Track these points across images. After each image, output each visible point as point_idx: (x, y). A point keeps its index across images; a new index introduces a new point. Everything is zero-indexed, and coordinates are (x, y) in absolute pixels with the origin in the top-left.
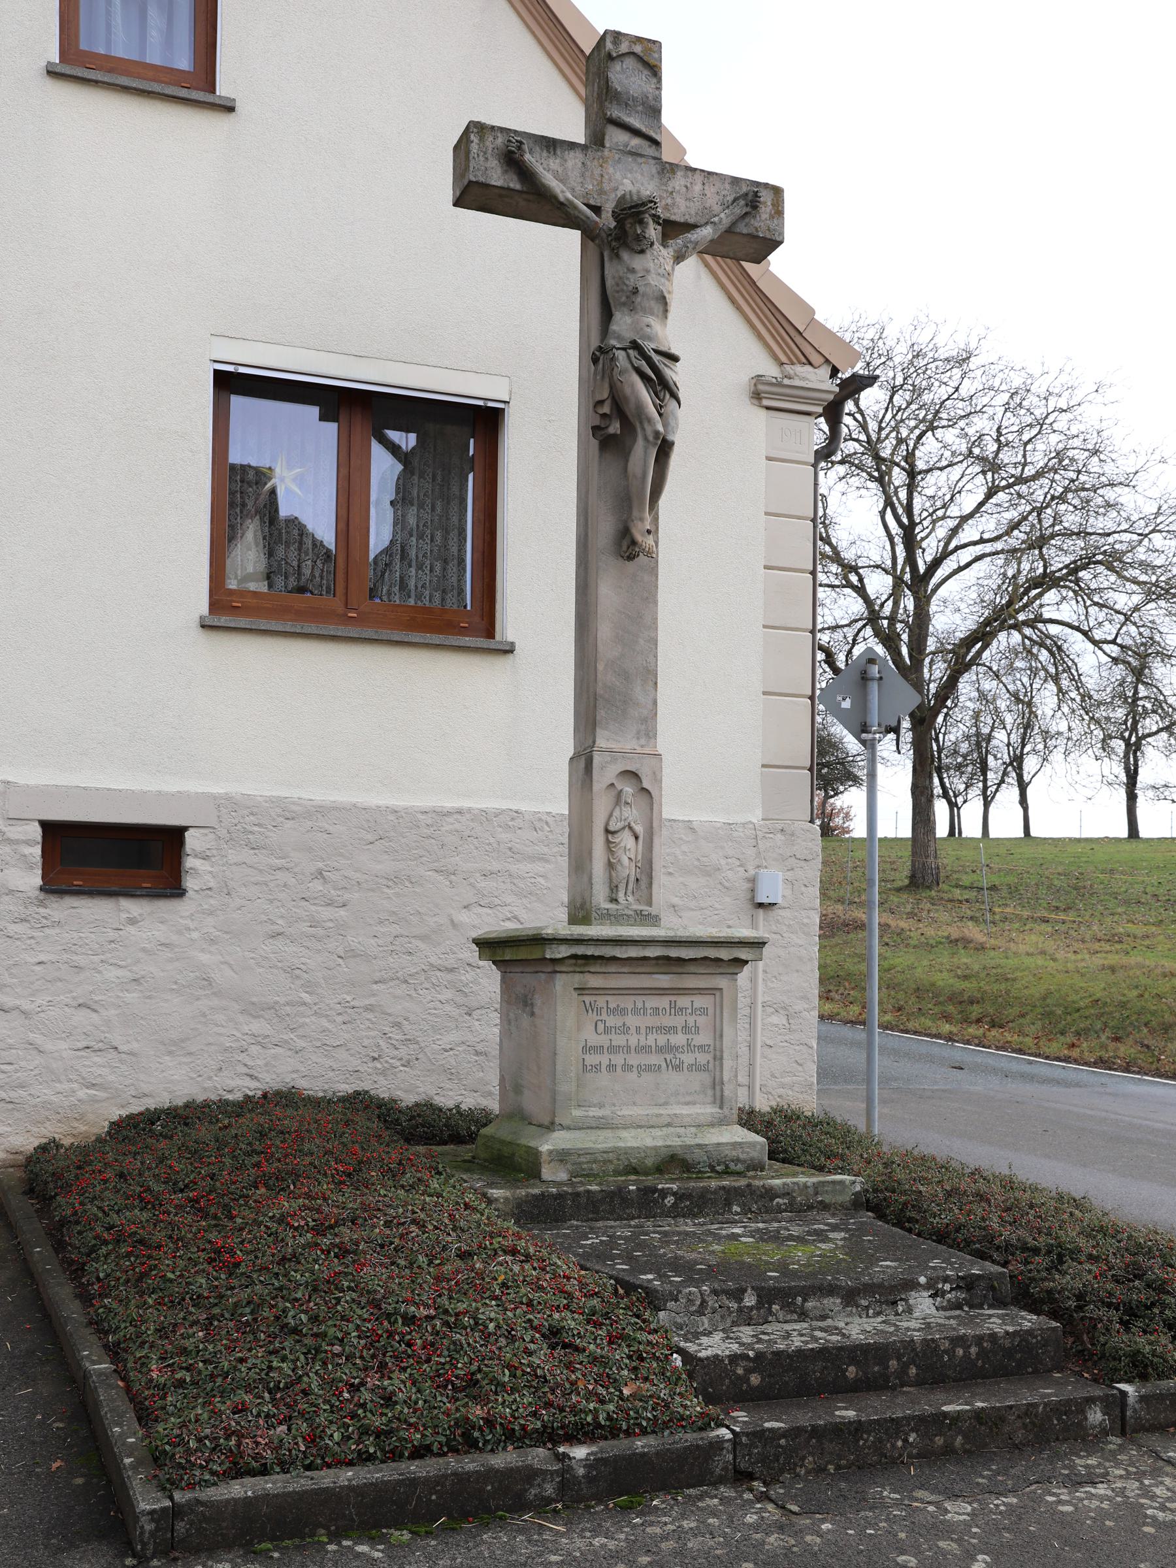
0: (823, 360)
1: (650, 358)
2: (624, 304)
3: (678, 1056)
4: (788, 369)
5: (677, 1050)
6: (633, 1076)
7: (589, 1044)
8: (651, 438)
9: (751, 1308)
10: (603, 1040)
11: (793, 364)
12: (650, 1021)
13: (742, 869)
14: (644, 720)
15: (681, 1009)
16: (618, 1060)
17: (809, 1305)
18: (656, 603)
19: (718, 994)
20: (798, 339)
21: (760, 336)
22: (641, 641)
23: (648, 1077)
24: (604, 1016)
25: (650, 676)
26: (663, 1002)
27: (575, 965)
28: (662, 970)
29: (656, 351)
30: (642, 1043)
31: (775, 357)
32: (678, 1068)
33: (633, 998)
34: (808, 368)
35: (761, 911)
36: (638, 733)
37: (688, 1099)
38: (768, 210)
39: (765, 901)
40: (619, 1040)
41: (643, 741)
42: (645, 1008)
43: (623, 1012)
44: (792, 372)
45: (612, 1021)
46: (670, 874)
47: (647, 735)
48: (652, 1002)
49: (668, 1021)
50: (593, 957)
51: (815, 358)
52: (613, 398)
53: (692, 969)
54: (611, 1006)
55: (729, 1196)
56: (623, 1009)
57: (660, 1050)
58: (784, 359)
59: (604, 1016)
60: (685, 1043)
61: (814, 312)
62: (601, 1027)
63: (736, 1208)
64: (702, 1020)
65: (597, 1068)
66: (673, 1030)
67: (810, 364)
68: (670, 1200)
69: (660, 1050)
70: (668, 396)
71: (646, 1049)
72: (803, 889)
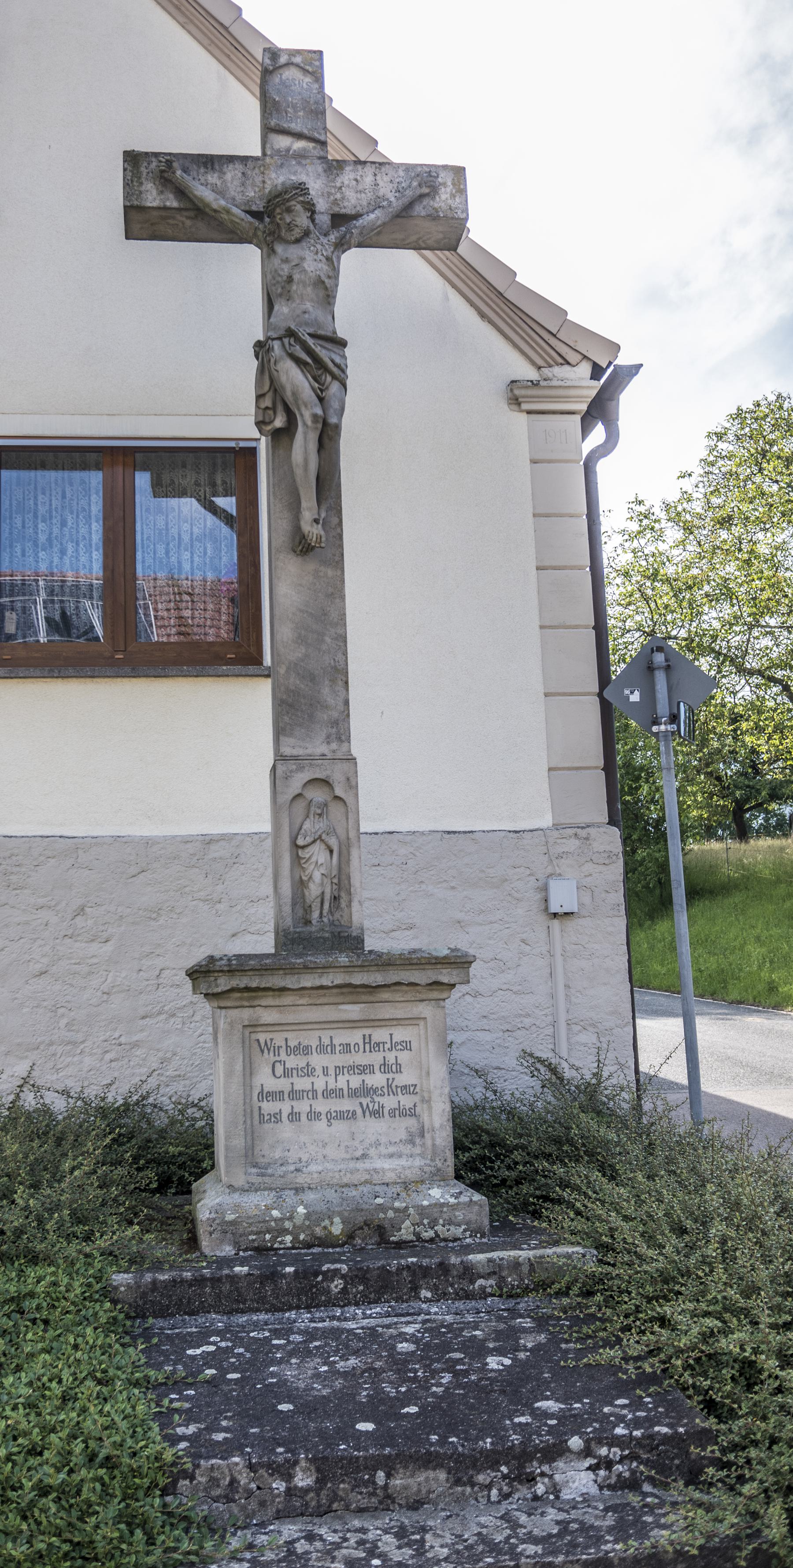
0: (580, 357)
1: (305, 341)
2: (281, 295)
3: (377, 1099)
4: (546, 372)
5: (375, 1092)
6: (321, 1125)
7: (295, 1088)
8: (309, 423)
9: (306, 1490)
10: (283, 1084)
11: (550, 366)
12: (340, 1059)
13: (533, 878)
14: (335, 723)
15: (378, 1044)
16: (303, 1107)
17: (397, 1482)
18: (343, 598)
19: (422, 1023)
20: (553, 341)
21: (515, 346)
22: (328, 639)
23: (340, 1128)
24: (283, 1056)
25: (340, 675)
26: (355, 1037)
27: (241, 999)
28: (347, 999)
29: (312, 335)
30: (332, 1086)
31: (533, 363)
32: (377, 1113)
33: (318, 1033)
34: (567, 368)
35: (556, 923)
36: (328, 737)
37: (392, 1149)
38: (448, 190)
39: (560, 911)
40: (302, 1084)
41: (334, 746)
42: (333, 1046)
43: (306, 1050)
44: (550, 375)
45: (292, 1062)
46: (453, 888)
47: (339, 739)
48: (342, 1037)
49: (361, 1059)
50: (257, 989)
51: (572, 357)
52: (275, 390)
53: (385, 995)
54: (292, 1043)
55: (420, 1274)
56: (307, 1047)
57: (354, 1093)
58: (540, 362)
59: (283, 1056)
60: (385, 1083)
61: (566, 313)
62: (279, 1069)
63: (425, 1293)
64: (404, 1057)
65: (276, 1117)
66: (367, 1069)
67: (568, 363)
68: (337, 1285)
69: (354, 1093)
70: (329, 378)
71: (337, 1093)
72: (604, 895)
